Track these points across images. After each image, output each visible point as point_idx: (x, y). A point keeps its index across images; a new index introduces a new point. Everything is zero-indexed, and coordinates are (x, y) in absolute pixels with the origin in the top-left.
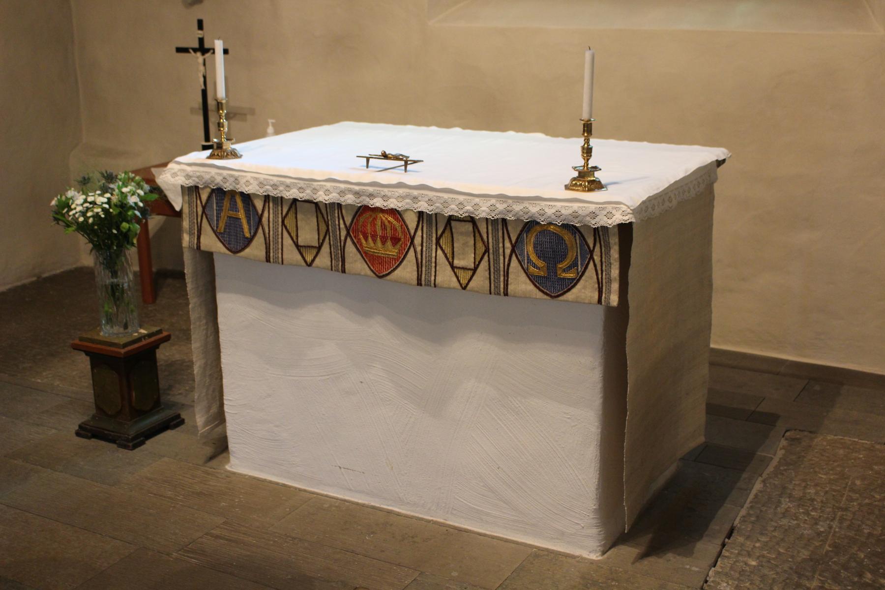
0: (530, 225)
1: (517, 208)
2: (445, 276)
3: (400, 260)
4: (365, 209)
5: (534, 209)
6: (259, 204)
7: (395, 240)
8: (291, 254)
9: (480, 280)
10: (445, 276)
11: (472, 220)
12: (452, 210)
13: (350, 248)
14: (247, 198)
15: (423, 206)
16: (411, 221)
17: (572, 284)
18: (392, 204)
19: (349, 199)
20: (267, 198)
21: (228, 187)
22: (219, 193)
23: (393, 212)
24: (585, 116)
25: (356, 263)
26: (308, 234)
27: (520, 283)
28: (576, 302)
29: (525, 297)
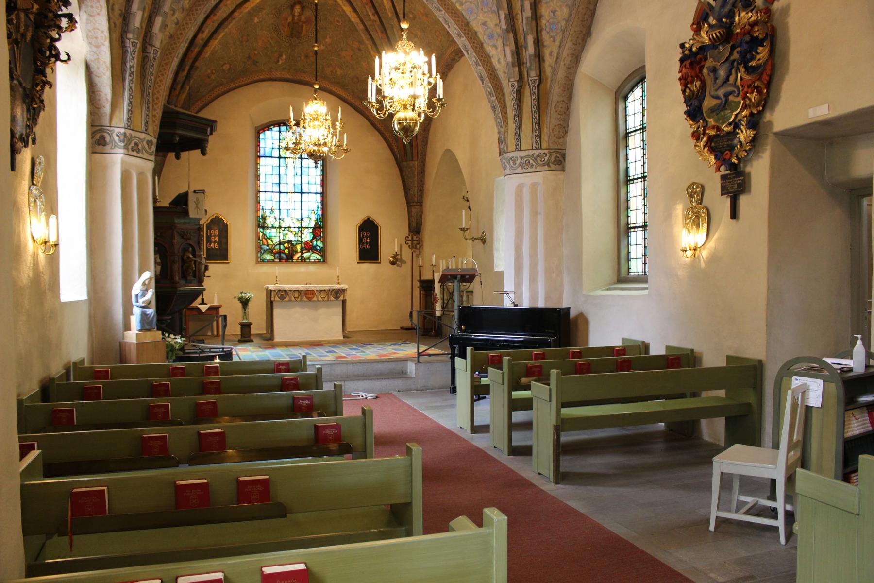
0: (333, 290)
1: (332, 288)
2: (320, 299)
3: (313, 298)
4: (308, 290)
5: (334, 288)
6: (288, 292)
7: (313, 294)
8: (293, 299)
9: (326, 299)
10: (320, 299)
11: (325, 290)
12: (322, 289)
13: (304, 297)
14: (285, 291)
15: (317, 289)
16: (315, 291)
17: (339, 297)
18: (313, 289)
19: (305, 289)
20: (289, 290)
21: (282, 289)
22: (280, 290)
23: (313, 290)
24: (338, 275)
25: (305, 299)
26: (296, 296)
27: (332, 298)
28: (340, 300)
29: (333, 301)
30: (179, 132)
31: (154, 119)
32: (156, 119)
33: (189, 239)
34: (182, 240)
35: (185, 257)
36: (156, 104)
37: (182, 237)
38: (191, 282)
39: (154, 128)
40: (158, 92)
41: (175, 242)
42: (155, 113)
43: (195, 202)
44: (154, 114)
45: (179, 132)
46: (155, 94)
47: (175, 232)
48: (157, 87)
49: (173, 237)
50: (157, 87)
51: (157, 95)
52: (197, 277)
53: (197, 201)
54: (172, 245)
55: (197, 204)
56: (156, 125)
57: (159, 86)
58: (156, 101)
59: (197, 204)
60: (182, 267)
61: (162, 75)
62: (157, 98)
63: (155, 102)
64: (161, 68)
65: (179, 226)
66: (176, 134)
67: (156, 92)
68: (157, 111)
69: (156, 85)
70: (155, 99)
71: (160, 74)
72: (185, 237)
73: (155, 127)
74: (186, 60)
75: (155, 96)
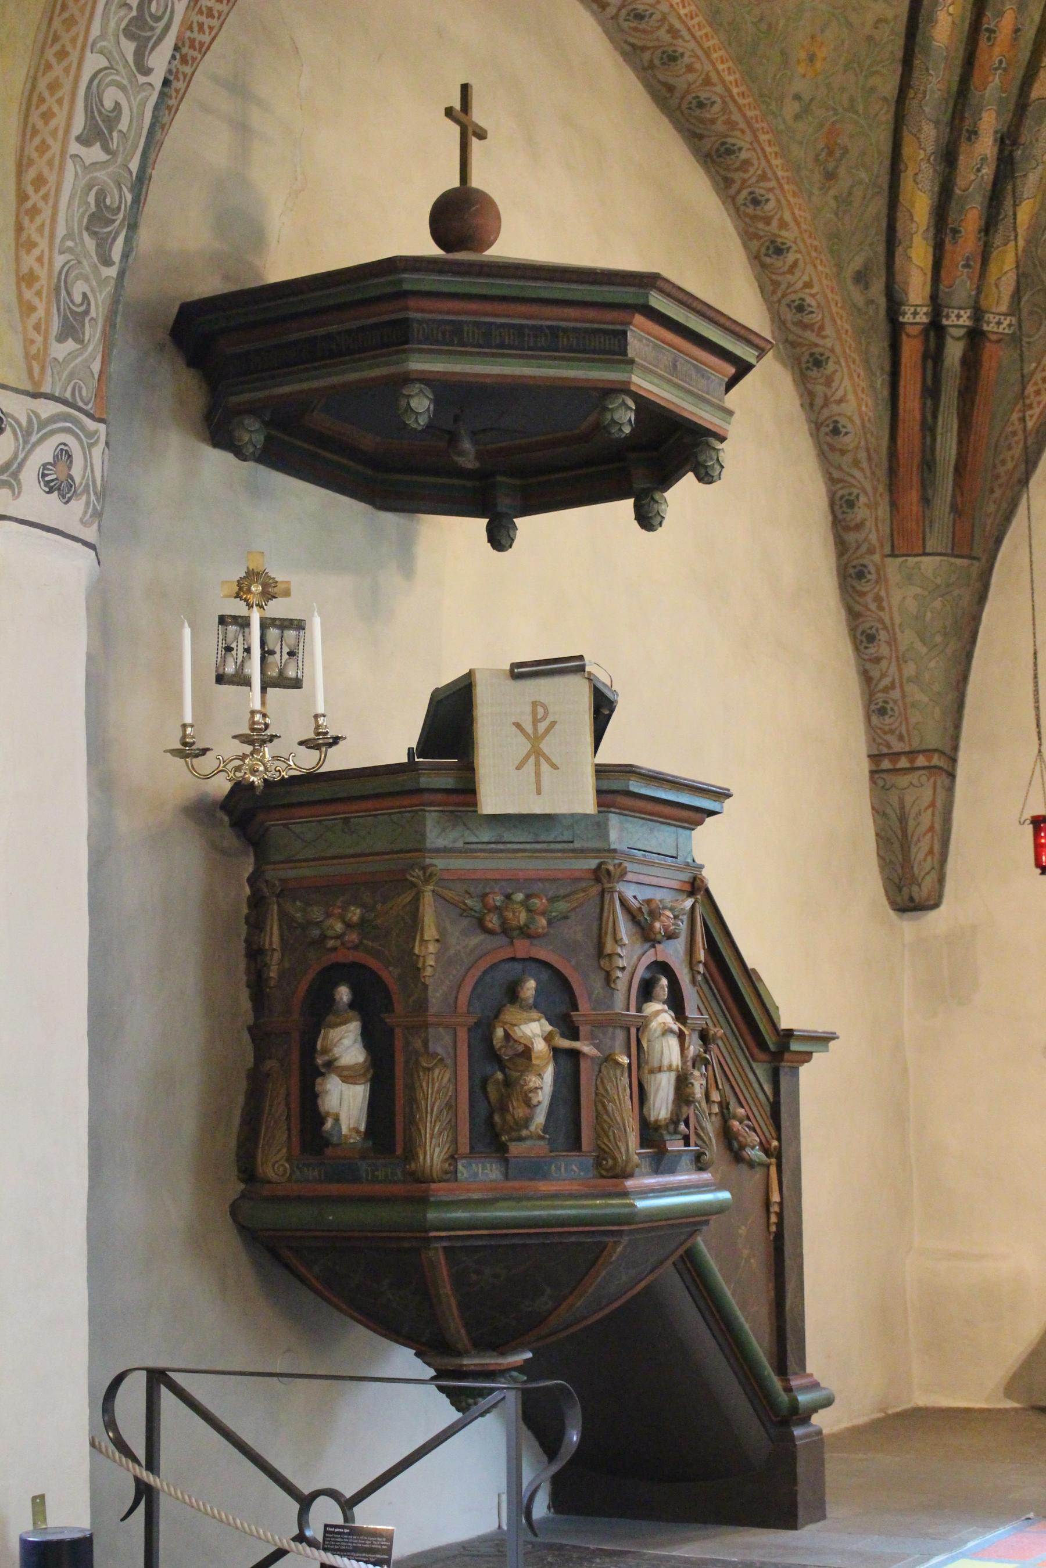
30: (418, 364)
31: (28, 294)
32: (38, 294)
33: (525, 932)
34: (476, 939)
35: (500, 1032)
36: (34, 211)
37: (482, 926)
38: (536, 1170)
39: (28, 342)
40: (43, 148)
41: (428, 952)
42: (29, 261)
43: (518, 725)
44: (25, 270)
45: (418, 364)
46: (31, 162)
47: (428, 900)
48: (40, 124)
49: (413, 924)
50: (40, 124)
51: (41, 165)
52: (585, 1147)
53: (535, 722)
54: (413, 969)
55: (535, 739)
56: (37, 327)
57: (47, 116)
58: (34, 198)
59: (535, 739)
60: (480, 1086)
61: (62, 54)
62: (39, 181)
63: (29, 204)
64: (57, 23)
65: (440, 863)
66: (407, 379)
67: (31, 150)
68: (36, 252)
69: (35, 118)
70: (30, 190)
71: (50, 54)
72: (493, 921)
73: (33, 335)
74: (976, 80)
75: (31, 174)
